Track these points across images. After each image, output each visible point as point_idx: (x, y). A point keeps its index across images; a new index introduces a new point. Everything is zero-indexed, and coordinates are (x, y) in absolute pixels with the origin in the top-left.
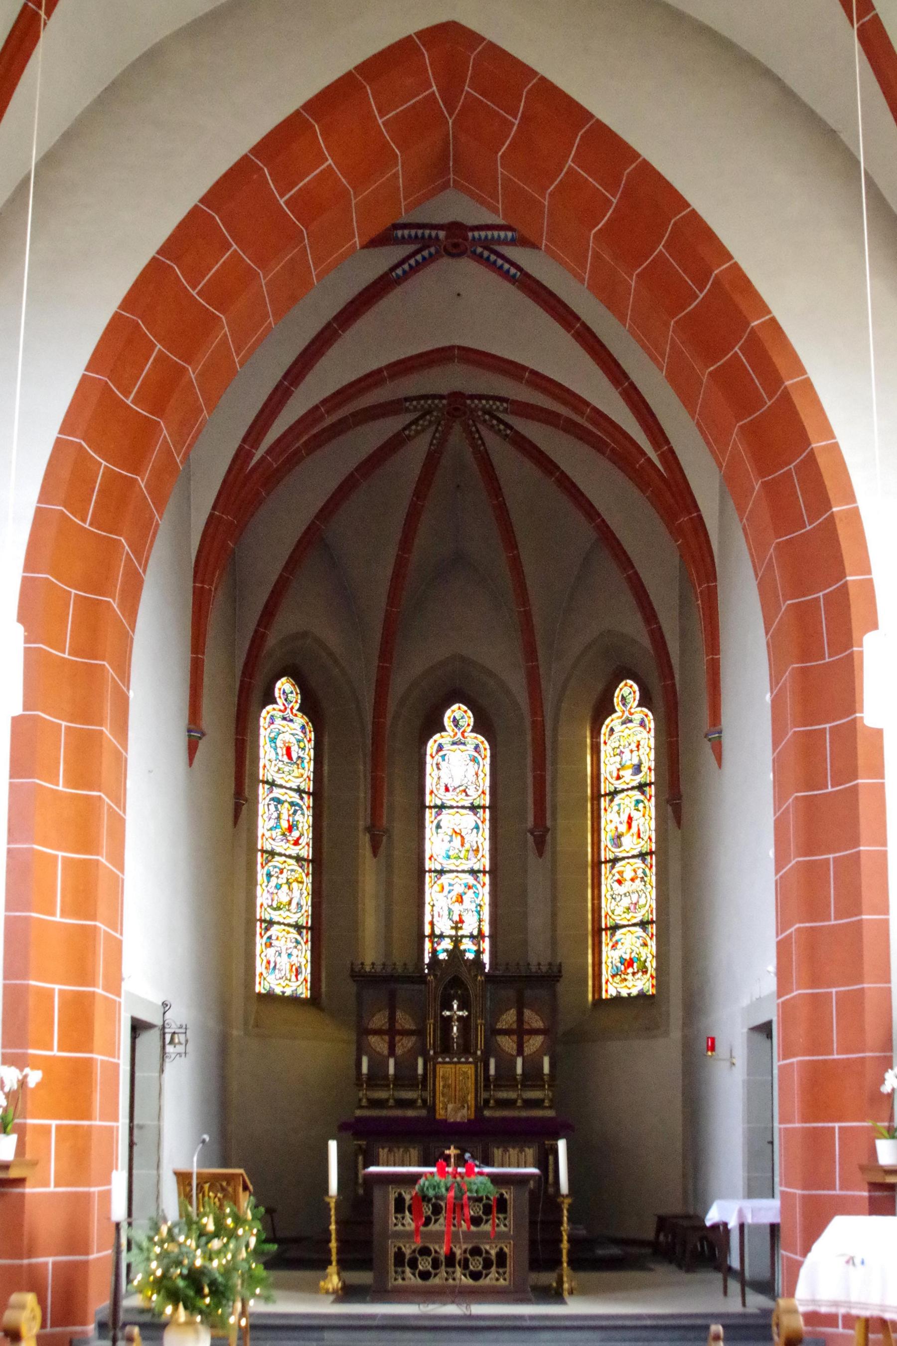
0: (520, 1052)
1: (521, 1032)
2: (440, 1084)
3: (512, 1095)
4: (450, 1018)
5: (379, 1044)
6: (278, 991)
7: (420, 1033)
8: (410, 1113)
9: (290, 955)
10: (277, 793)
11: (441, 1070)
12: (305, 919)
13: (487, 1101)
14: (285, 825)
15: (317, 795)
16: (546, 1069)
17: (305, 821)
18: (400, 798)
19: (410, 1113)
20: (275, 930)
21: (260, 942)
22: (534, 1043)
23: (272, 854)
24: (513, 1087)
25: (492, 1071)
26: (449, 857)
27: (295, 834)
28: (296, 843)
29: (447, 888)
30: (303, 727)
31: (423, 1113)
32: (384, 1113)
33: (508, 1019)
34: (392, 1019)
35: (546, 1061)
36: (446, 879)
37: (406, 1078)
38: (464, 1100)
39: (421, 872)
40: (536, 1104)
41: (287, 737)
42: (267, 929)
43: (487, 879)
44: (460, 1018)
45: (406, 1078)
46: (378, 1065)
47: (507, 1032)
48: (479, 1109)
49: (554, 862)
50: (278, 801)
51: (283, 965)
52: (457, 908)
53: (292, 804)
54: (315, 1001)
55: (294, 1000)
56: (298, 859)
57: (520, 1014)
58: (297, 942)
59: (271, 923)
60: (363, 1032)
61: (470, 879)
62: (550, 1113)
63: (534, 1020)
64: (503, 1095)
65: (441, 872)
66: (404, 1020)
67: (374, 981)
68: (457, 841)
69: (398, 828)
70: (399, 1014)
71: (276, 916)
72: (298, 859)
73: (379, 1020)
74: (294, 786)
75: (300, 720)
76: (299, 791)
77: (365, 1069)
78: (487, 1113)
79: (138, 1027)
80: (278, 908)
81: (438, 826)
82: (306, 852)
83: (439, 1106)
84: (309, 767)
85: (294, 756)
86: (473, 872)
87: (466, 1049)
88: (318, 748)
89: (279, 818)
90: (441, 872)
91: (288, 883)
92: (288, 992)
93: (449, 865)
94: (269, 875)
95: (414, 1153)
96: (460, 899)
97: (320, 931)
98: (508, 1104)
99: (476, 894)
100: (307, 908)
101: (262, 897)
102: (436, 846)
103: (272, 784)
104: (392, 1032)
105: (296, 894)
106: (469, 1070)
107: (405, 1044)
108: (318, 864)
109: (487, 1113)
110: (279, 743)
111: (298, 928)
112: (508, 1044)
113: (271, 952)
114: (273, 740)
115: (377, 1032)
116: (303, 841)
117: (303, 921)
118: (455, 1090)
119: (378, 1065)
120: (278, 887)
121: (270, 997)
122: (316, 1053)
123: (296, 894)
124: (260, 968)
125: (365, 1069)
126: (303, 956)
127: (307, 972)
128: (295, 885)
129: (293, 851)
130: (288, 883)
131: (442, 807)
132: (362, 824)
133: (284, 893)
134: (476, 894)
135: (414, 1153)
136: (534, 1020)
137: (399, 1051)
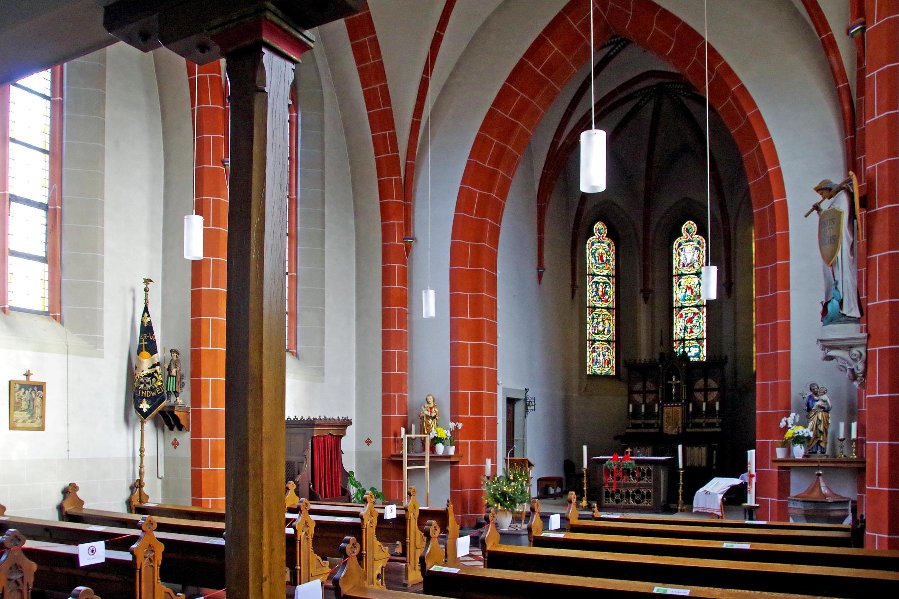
0: (706, 400)
1: (706, 390)
2: (665, 416)
3: (702, 421)
4: (671, 385)
5: (638, 398)
6: (599, 372)
7: (657, 392)
8: (652, 430)
9: (604, 355)
10: (596, 278)
11: (666, 410)
12: (612, 337)
13: (688, 424)
14: (600, 293)
15: (617, 276)
16: (717, 408)
17: (611, 290)
18: (657, 274)
19: (652, 430)
20: (596, 345)
21: (589, 351)
22: (713, 395)
23: (595, 308)
24: (701, 417)
25: (691, 410)
26: (685, 300)
27: (607, 297)
28: (607, 301)
29: (684, 316)
30: (609, 245)
31: (657, 430)
32: (639, 431)
33: (700, 383)
34: (644, 386)
35: (717, 404)
36: (683, 312)
37: (650, 413)
38: (677, 424)
39: (671, 308)
40: (712, 425)
41: (601, 250)
42: (592, 344)
43: (705, 310)
44: (677, 385)
45: (650, 413)
46: (637, 408)
47: (699, 390)
48: (684, 428)
49: (735, 299)
50: (597, 282)
51: (601, 360)
52: (689, 325)
53: (604, 283)
54: (617, 377)
55: (607, 376)
56: (608, 309)
57: (706, 382)
58: (608, 349)
59: (595, 341)
60: (631, 392)
61: (696, 310)
62: (719, 430)
63: (712, 384)
64: (697, 421)
65: (682, 308)
66: (650, 386)
67: (649, 367)
68: (689, 292)
69: (658, 289)
70: (648, 383)
71: (597, 337)
72: (608, 309)
73: (638, 386)
74: (604, 273)
75: (608, 241)
76: (608, 276)
77: (631, 410)
78: (688, 430)
79: (511, 402)
80: (598, 334)
81: (680, 285)
82: (612, 305)
83: (665, 426)
84: (613, 263)
85: (605, 259)
86: (697, 307)
87: (678, 400)
88: (617, 254)
89: (597, 290)
90: (682, 308)
91: (603, 321)
92: (604, 373)
93: (685, 304)
94: (593, 319)
95: (649, 450)
96: (690, 321)
97: (620, 342)
98: (699, 425)
99: (699, 318)
100: (613, 332)
101: (590, 329)
102: (678, 294)
103: (594, 275)
104: (644, 392)
105: (607, 325)
106: (679, 409)
107: (650, 398)
108: (620, 310)
109: (688, 430)
110: (597, 254)
111: (608, 342)
112: (699, 396)
113: (595, 354)
114: (593, 254)
115: (638, 392)
116: (611, 300)
117: (611, 339)
118: (672, 418)
119: (637, 408)
120: (598, 323)
121: (595, 376)
122: (615, 403)
123: (607, 325)
124: (589, 362)
125: (631, 410)
126: (611, 355)
127: (613, 363)
128: (606, 322)
129: (605, 305)
130: (603, 321)
131: (682, 275)
132: (639, 289)
133: (601, 326)
134: (699, 318)
135: (649, 450)
136: (712, 384)
137: (648, 401)
